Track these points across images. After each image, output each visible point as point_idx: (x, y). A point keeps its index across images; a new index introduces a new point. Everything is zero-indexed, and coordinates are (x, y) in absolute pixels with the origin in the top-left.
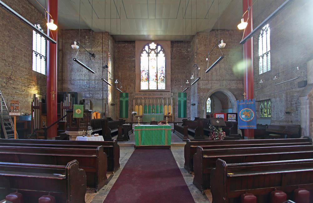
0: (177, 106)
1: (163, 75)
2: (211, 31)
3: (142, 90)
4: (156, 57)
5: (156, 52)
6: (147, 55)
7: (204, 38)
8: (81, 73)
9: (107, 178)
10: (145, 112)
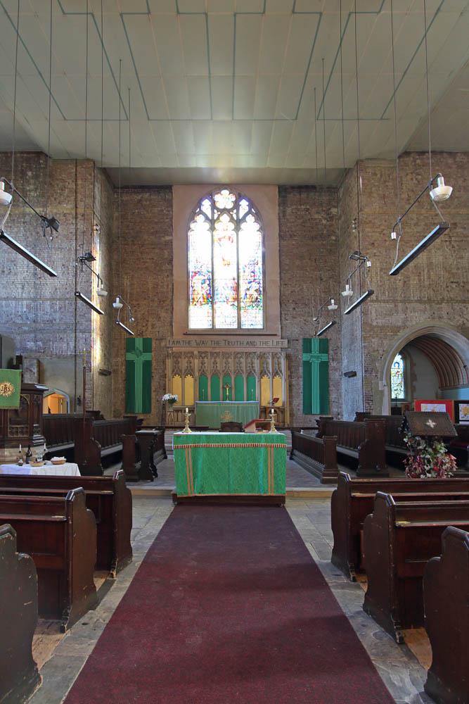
0: (301, 379)
1: (255, 286)
2: (400, 157)
4: (234, 233)
5: (235, 216)
6: (207, 225)
7: (379, 176)
8: (12, 278)
9: (95, 587)
10: (202, 396)
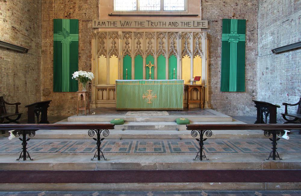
3: (117, 12)
10: (126, 75)
